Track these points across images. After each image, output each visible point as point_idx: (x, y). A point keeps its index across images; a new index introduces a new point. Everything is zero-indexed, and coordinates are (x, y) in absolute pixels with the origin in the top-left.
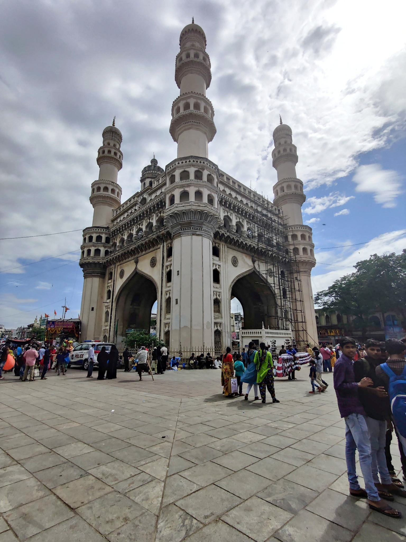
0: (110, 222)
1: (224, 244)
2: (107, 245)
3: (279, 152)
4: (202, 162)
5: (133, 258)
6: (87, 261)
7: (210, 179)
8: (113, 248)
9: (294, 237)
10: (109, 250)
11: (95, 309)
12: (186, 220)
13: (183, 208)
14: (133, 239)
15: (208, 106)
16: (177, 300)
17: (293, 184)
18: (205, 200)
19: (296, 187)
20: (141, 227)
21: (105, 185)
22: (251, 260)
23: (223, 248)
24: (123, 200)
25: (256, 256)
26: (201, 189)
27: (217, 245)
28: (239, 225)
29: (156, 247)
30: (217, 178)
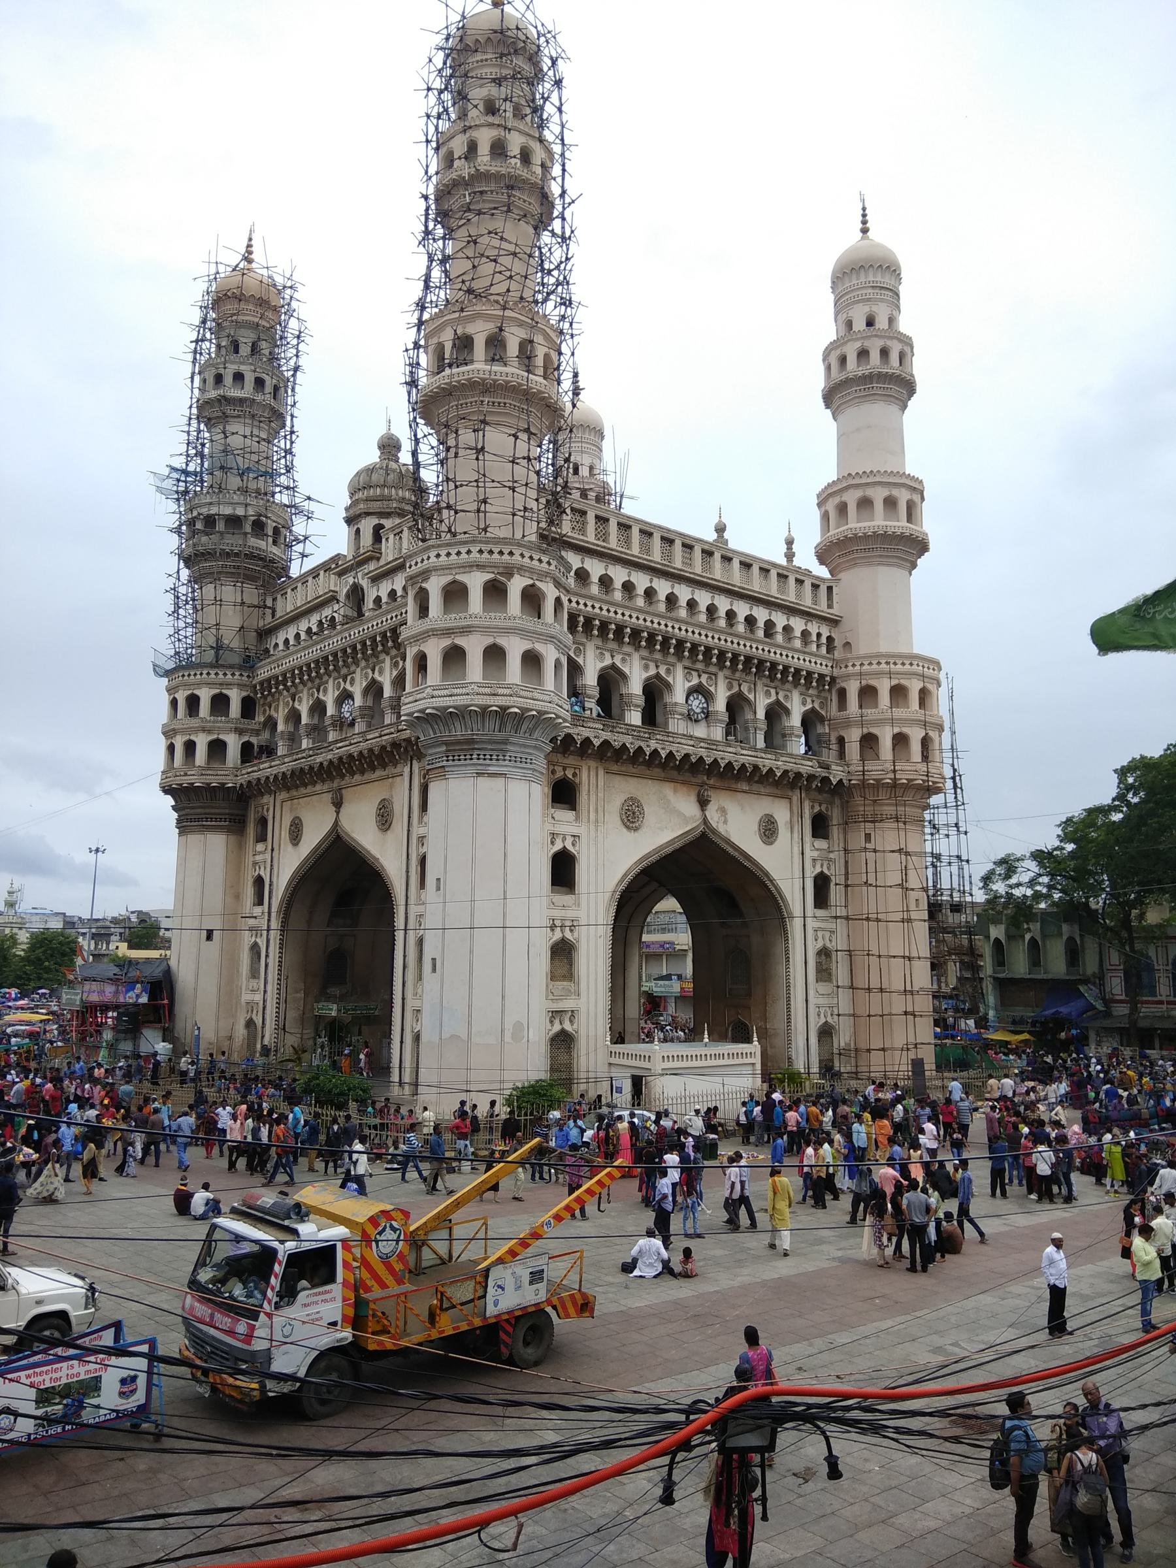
1: (593, 764)
4: (506, 551)
5: (326, 787)
6: (185, 781)
8: (266, 735)
9: (868, 693)
10: (254, 740)
12: (459, 732)
13: (448, 701)
16: (434, 960)
20: (348, 687)
22: (693, 799)
23: (592, 781)
25: (712, 782)
26: (502, 641)
28: (654, 692)
29: (390, 770)
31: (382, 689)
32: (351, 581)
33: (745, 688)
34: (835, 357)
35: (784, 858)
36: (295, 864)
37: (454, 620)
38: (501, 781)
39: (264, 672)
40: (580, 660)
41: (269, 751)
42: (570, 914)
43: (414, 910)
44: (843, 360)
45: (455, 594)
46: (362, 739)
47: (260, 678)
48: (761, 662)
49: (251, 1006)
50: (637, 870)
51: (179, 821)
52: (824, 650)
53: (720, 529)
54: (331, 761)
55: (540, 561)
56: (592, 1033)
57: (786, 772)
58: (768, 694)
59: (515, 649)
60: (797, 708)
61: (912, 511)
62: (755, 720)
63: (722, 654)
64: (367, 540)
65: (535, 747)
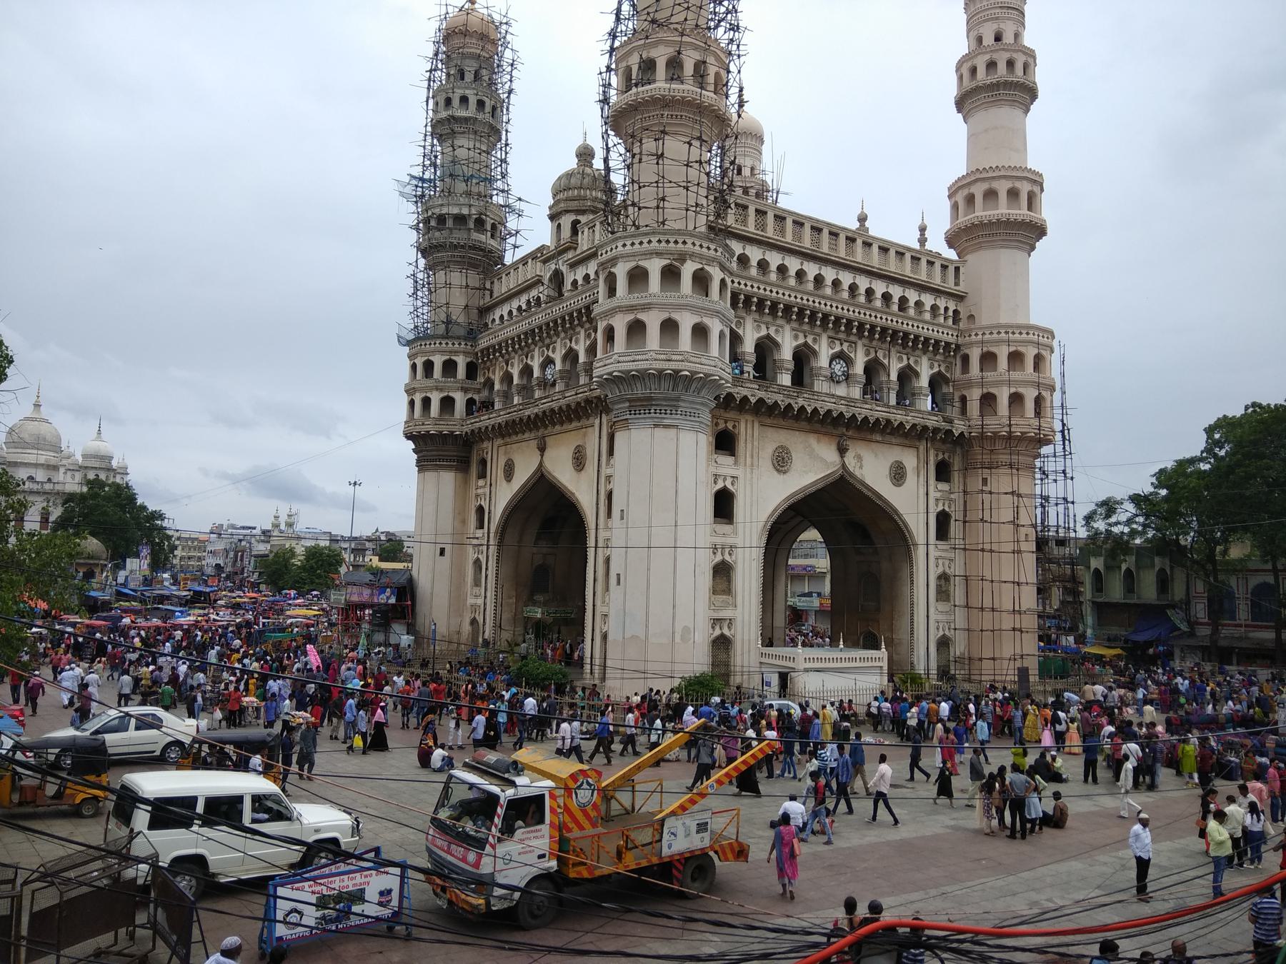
1: (749, 418)
2: (469, 384)
4: (680, 241)
6: (423, 429)
8: (485, 393)
9: (988, 359)
10: (476, 397)
11: (447, 552)
12: (639, 391)
16: (618, 575)
20: (550, 354)
22: (834, 447)
23: (748, 432)
25: (850, 433)
27: (730, 426)
28: (802, 358)
29: (584, 422)
32: (553, 267)
33: (880, 355)
34: (966, 68)
35: (912, 499)
36: (509, 496)
37: (637, 298)
38: (673, 431)
39: (484, 343)
40: (740, 332)
41: (487, 405)
42: (729, 541)
44: (974, 71)
45: (638, 277)
46: (562, 397)
47: (481, 347)
48: (895, 332)
49: (474, 608)
50: (786, 506)
51: (418, 461)
52: (950, 321)
53: (862, 219)
54: (537, 415)
55: (708, 248)
56: (746, 638)
57: (914, 425)
58: (900, 359)
59: (686, 322)
60: (925, 372)
61: (1032, 201)
63: (861, 326)
64: (566, 232)
65: (702, 404)
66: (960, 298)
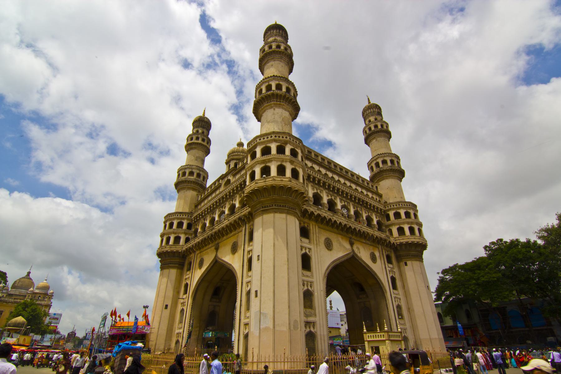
0: (193, 207)
1: (314, 223)
2: (188, 231)
3: (370, 129)
5: (213, 244)
6: (165, 250)
7: (294, 153)
9: (397, 215)
10: (190, 237)
11: (169, 307)
14: (215, 223)
15: (290, 87)
16: (256, 292)
17: (388, 159)
18: (288, 173)
19: (392, 161)
21: (190, 170)
22: (348, 242)
23: (313, 228)
24: (209, 183)
26: (284, 164)
27: (306, 225)
30: (302, 152)
31: (235, 206)
32: (226, 179)
43: (245, 280)
48: (363, 201)
50: (332, 266)
56: (322, 334)
58: (366, 213)
62: (363, 220)
64: (232, 166)
66: (380, 196)
